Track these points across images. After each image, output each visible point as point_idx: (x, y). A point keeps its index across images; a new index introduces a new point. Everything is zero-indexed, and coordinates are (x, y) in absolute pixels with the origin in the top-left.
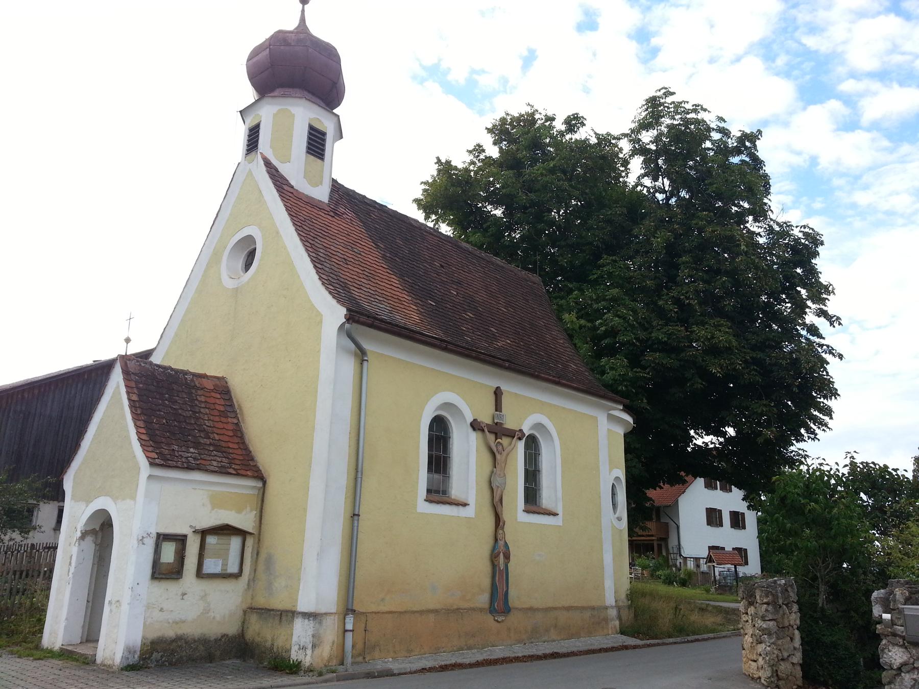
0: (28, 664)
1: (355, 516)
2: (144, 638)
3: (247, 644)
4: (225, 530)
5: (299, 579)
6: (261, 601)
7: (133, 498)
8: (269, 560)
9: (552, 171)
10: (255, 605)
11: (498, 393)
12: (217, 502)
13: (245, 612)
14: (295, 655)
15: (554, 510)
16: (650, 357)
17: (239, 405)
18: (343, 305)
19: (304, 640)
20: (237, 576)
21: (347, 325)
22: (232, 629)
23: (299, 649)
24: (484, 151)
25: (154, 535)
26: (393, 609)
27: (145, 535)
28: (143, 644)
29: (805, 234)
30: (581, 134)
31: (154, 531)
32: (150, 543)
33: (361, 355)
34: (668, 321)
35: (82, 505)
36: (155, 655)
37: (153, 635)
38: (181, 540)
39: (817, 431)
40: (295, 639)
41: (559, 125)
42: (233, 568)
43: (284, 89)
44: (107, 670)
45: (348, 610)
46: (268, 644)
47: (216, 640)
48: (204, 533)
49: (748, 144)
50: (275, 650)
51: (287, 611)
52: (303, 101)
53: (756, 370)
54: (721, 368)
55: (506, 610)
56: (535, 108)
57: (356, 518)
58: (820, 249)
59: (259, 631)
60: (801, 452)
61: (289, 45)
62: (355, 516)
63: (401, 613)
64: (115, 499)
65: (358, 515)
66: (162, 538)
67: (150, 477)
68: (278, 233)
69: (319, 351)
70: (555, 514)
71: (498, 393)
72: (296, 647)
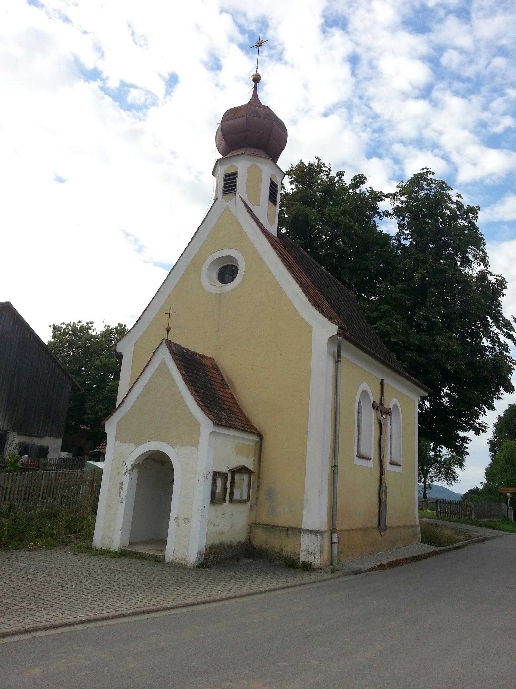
0: (84, 558)
1: (335, 467)
2: (206, 545)
3: (255, 548)
4: (243, 470)
5: (302, 507)
6: (265, 519)
7: (195, 444)
8: (270, 494)
9: (344, 213)
10: (258, 521)
11: (382, 383)
12: (239, 451)
13: (250, 526)
14: (303, 558)
15: (399, 463)
16: (410, 354)
17: (228, 378)
18: (335, 323)
19: (313, 548)
20: (248, 500)
21: (340, 338)
22: (242, 538)
23: (308, 554)
24: (284, 188)
25: (212, 473)
26: (346, 529)
27: (208, 473)
28: (206, 549)
29: (497, 280)
30: (364, 188)
31: (211, 470)
32: (210, 477)
33: (337, 359)
34: (420, 331)
35: (132, 447)
36: (211, 557)
37: (210, 543)
38: (224, 475)
39: (486, 410)
40: (303, 547)
41: (348, 180)
42: (245, 497)
43: (256, 150)
44: (180, 567)
45: (332, 530)
46: (277, 549)
47: (237, 545)
48: (233, 472)
49: (471, 215)
50: (283, 553)
51: (292, 528)
52: (265, 160)
53: (470, 369)
54: (452, 366)
55: (385, 528)
56: (322, 162)
57: (336, 468)
58: (504, 291)
59: (261, 538)
60: (484, 424)
61: (259, 116)
62: (335, 467)
63: (349, 530)
64: (173, 445)
65: (337, 466)
66: (216, 475)
67: (213, 433)
68: (261, 259)
69: (310, 352)
70: (400, 465)
71: (382, 383)
72: (305, 553)
